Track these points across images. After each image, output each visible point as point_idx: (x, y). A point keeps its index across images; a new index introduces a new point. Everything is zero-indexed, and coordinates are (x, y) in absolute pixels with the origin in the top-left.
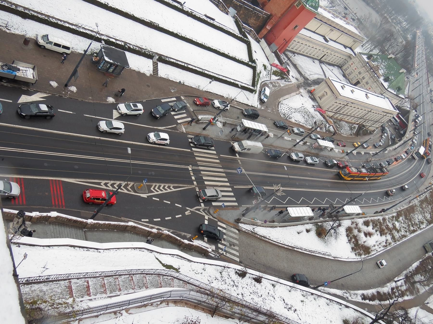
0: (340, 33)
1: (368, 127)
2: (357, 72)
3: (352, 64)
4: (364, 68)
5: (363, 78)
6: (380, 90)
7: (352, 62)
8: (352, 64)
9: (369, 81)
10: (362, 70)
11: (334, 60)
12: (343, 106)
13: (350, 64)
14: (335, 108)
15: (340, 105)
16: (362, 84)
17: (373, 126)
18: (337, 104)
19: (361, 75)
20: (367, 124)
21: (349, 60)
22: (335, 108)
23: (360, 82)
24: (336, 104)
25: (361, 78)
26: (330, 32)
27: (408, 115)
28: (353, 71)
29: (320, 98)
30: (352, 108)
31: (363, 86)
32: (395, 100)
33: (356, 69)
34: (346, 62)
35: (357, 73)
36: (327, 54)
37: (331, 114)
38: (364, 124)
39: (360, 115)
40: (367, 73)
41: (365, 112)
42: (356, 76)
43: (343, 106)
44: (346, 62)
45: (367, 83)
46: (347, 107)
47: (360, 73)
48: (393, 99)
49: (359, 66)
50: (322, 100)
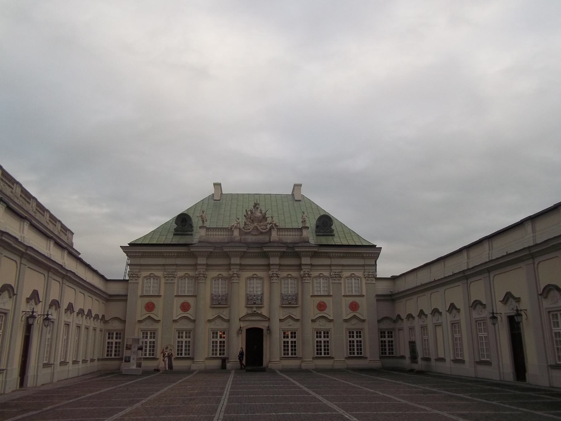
3: (150, 307)
4: (214, 274)
7: (141, 304)
8: (150, 307)
9: (289, 288)
13: (140, 313)
16: (276, 327)
21: (115, 309)
23: (263, 325)
25: (243, 311)
33: (185, 307)
34: (116, 325)
35: (211, 314)
45: (290, 302)
47: (221, 302)
49: (187, 287)
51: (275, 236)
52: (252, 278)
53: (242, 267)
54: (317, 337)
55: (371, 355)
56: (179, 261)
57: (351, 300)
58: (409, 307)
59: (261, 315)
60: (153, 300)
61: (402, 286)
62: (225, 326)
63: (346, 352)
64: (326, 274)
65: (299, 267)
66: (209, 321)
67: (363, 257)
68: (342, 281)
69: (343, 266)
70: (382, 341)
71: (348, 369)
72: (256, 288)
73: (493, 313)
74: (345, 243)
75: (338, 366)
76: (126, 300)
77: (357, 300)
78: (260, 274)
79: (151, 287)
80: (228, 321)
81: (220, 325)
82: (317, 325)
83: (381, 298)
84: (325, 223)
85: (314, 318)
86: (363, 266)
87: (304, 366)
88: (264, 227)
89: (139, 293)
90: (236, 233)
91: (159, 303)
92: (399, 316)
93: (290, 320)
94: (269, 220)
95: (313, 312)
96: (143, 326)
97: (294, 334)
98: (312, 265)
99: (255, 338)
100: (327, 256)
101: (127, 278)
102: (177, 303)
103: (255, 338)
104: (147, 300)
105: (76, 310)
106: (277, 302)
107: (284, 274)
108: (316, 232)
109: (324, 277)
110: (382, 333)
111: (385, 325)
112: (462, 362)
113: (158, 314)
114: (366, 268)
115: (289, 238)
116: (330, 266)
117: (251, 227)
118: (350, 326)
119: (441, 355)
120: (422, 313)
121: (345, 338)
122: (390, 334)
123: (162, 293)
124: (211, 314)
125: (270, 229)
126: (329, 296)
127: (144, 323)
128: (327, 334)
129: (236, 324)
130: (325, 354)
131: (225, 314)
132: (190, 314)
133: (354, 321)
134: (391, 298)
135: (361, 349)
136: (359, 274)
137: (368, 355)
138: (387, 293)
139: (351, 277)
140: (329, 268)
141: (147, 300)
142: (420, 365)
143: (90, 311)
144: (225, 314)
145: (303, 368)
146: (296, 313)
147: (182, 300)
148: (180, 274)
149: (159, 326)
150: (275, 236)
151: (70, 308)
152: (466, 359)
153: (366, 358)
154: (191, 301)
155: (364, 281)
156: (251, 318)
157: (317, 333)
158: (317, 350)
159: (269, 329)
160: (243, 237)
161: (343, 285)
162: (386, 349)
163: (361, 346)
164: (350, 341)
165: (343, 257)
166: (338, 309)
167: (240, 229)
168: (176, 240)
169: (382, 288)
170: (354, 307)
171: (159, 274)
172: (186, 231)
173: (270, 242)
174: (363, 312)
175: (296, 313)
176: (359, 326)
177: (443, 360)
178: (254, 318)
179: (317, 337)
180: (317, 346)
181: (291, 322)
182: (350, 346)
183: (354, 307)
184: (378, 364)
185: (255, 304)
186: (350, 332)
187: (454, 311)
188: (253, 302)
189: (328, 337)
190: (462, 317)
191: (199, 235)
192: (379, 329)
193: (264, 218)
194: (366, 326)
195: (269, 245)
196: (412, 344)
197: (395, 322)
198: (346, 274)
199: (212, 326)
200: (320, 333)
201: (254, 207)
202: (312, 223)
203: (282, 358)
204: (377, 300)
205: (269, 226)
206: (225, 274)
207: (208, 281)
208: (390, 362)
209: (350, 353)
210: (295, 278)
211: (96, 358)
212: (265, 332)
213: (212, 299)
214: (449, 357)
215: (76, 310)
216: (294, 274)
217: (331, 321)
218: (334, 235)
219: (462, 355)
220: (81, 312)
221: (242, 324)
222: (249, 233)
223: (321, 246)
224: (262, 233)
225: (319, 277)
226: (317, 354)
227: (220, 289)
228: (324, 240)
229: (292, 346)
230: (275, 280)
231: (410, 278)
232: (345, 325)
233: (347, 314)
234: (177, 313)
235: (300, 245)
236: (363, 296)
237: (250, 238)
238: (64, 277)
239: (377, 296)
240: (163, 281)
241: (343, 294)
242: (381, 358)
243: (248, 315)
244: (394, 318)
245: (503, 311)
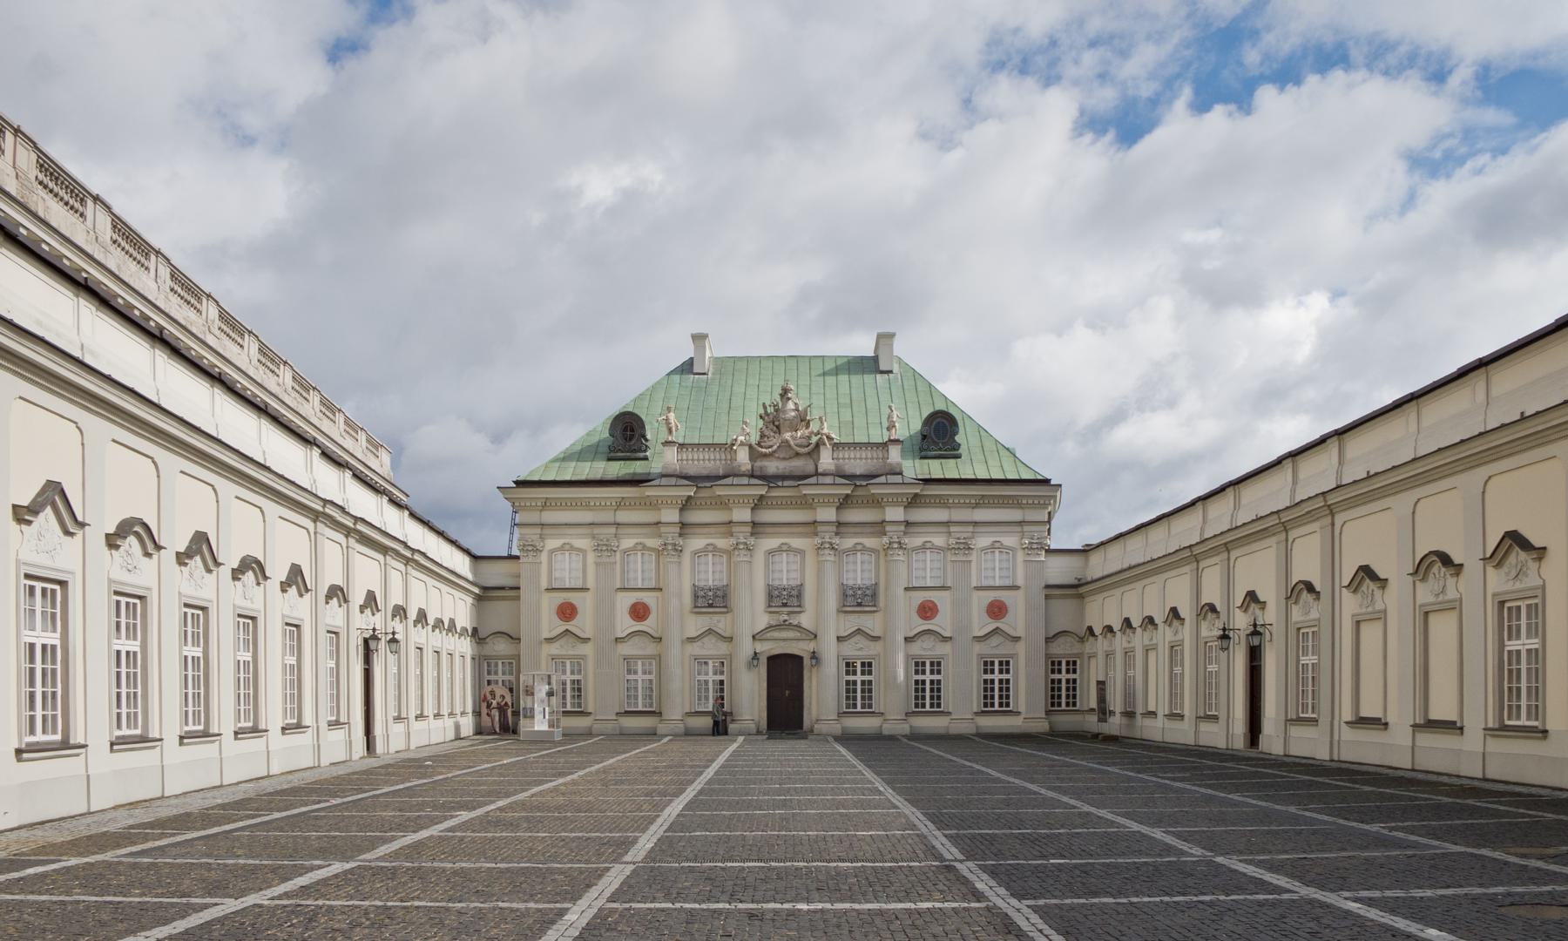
3: (567, 612)
4: (697, 543)
7: (549, 603)
8: (567, 612)
9: (859, 573)
10: (698, 565)
13: (550, 624)
16: (830, 651)
25: (763, 621)
33: (639, 612)
35: (695, 625)
42: (710, 648)
44: (501, 647)
45: (859, 600)
47: (713, 600)
49: (641, 570)
51: (826, 460)
52: (779, 550)
53: (757, 528)
54: (917, 672)
55: (1028, 708)
56: (624, 516)
57: (991, 596)
58: (1104, 610)
59: (798, 627)
60: (573, 598)
61: (1098, 566)
62: (723, 648)
63: (976, 703)
64: (939, 541)
65: (879, 527)
66: (691, 640)
67: (1020, 506)
68: (973, 557)
69: (976, 523)
70: (1053, 681)
71: (978, 735)
72: (786, 574)
73: (1255, 625)
74: (982, 474)
75: (957, 728)
76: (518, 598)
77: (1002, 595)
78: (796, 543)
79: (567, 570)
80: (730, 639)
81: (710, 648)
82: (917, 649)
83: (1053, 590)
84: (940, 431)
85: (912, 634)
86: (1021, 523)
87: (888, 729)
88: (804, 442)
89: (544, 584)
90: (743, 456)
91: (585, 604)
92: (1090, 629)
93: (858, 637)
94: (814, 427)
95: (905, 620)
96: (554, 649)
97: (867, 667)
98: (908, 524)
99: (785, 677)
100: (942, 503)
101: (515, 552)
102: (625, 601)
103: (785, 677)
104: (561, 597)
105: (431, 621)
106: (832, 601)
107: (849, 543)
108: (921, 450)
109: (934, 548)
110: (1054, 666)
111: (1062, 649)
112: (1182, 717)
113: (584, 623)
114: (1026, 528)
115: (858, 463)
116: (947, 524)
117: (775, 442)
118: (986, 649)
119: (1151, 708)
120: (1127, 623)
121: (976, 677)
122: (1072, 666)
123: (590, 583)
124: (695, 625)
125: (817, 445)
126: (943, 588)
127: (557, 645)
128: (936, 667)
129: (746, 648)
130: (932, 705)
132: (648, 625)
133: (995, 640)
134: (1077, 590)
135: (1008, 697)
136: (1010, 540)
137: (1022, 708)
138: (1070, 580)
139: (993, 547)
140: (944, 529)
141: (561, 597)
142: (1115, 725)
143: (452, 621)
144: (721, 623)
145: (885, 732)
146: (872, 623)
147: (630, 598)
148: (627, 543)
149: (587, 650)
151: (422, 617)
152: (1187, 713)
153: (1019, 713)
154: (648, 598)
155: (1020, 556)
156: (776, 634)
157: (917, 664)
158: (917, 698)
159: (814, 656)
160: (758, 464)
161: (974, 565)
162: (1059, 695)
163: (1008, 689)
164: (985, 681)
165: (977, 506)
166: (963, 616)
167: (750, 447)
168: (616, 469)
169: (1059, 570)
170: (997, 610)
171: (583, 543)
172: (635, 451)
173: (817, 474)
174: (1017, 620)
175: (872, 623)
176: (1006, 649)
177: (1153, 714)
178: (784, 634)
179: (917, 672)
180: (917, 690)
181: (859, 641)
182: (985, 690)
183: (997, 610)
184: (1042, 726)
185: (785, 605)
186: (986, 663)
187: (1176, 623)
188: (784, 599)
189: (939, 672)
190: (1186, 633)
191: (662, 459)
192: (1047, 656)
193: (803, 419)
194: (1020, 649)
195: (812, 480)
196: (1101, 685)
197: (1082, 640)
198: (983, 541)
199: (696, 649)
200: (924, 664)
201: (782, 396)
202: (910, 424)
203: (841, 714)
204: (1047, 597)
205: (814, 439)
206: (722, 543)
207: (686, 558)
208: (1065, 721)
209: (986, 705)
210: (873, 550)
212: (807, 662)
213: (696, 597)
214: (1163, 709)
215: (431, 621)
216: (870, 542)
217: (946, 639)
218: (958, 457)
219: (1182, 708)
220: (439, 623)
221: (760, 647)
222: (771, 455)
223: (927, 481)
224: (797, 454)
225: (923, 548)
226: (917, 706)
227: (711, 574)
228: (936, 468)
229: (863, 691)
230: (829, 556)
231: (1114, 551)
232: (978, 648)
233: (981, 624)
234: (625, 624)
235: (882, 479)
236: (1017, 588)
237: (772, 467)
238: (407, 561)
239: (1048, 587)
240: (591, 558)
241: (974, 584)
242: (1048, 713)
243: (770, 628)
244: (1083, 631)
245: (1241, 621)
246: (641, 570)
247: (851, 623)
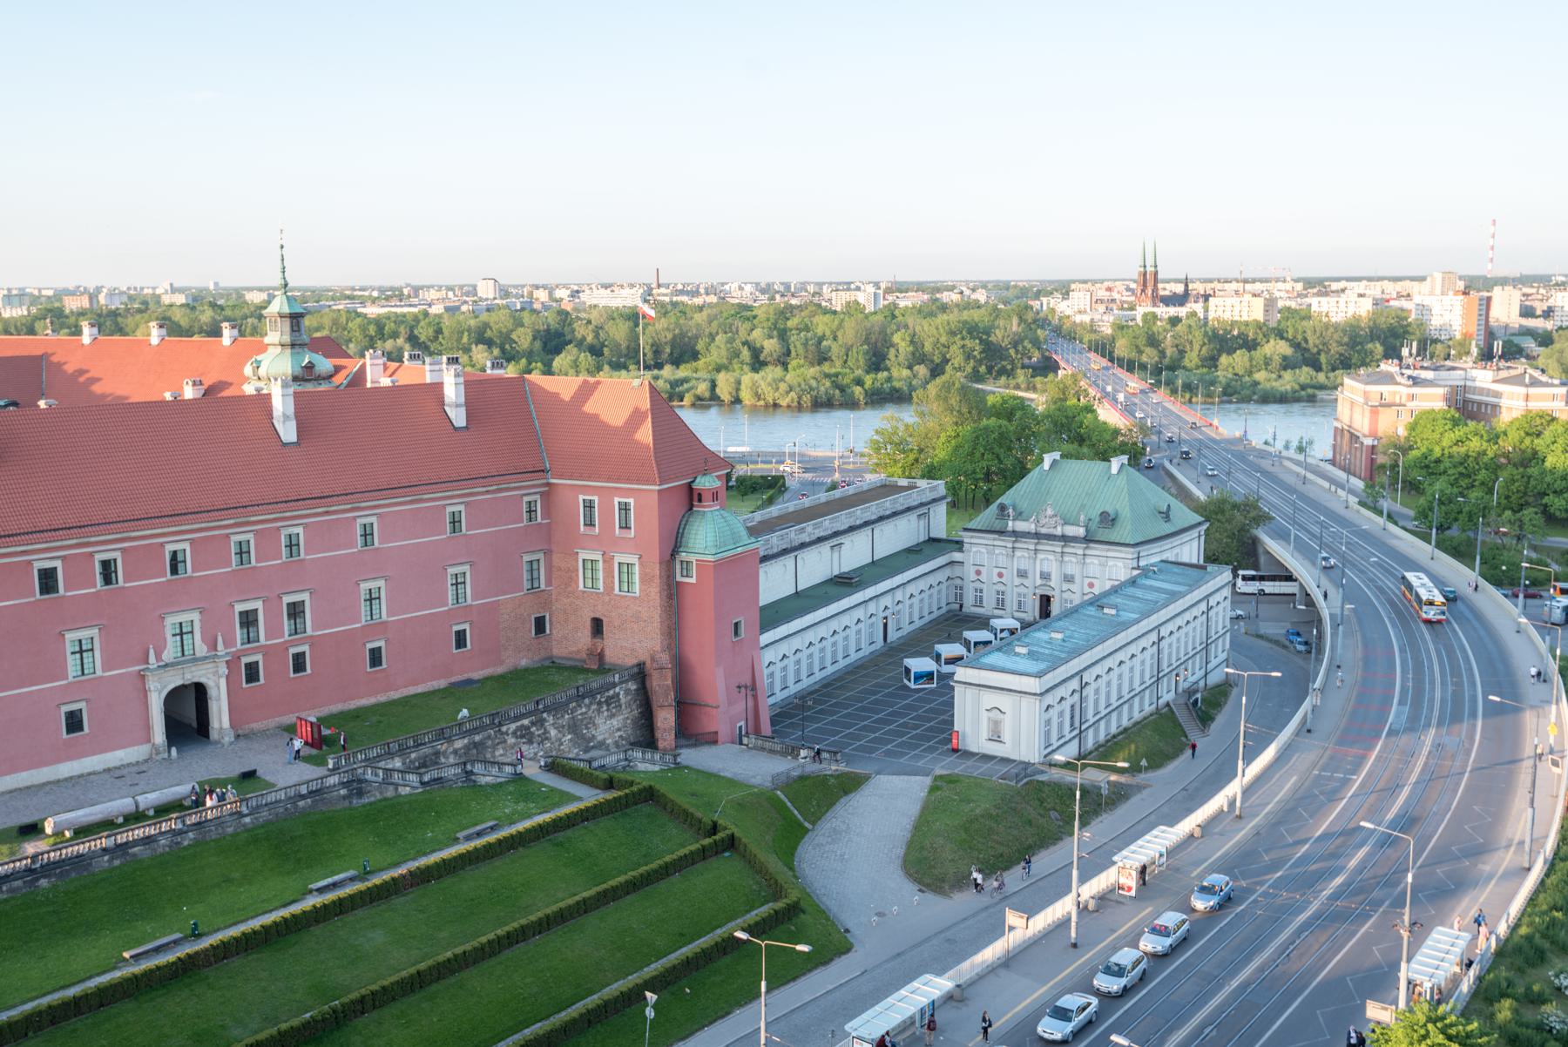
0: (867, 531)
1: (1202, 684)
2: (1011, 578)
3: (978, 573)
5: (1045, 576)
6: (1120, 564)
7: (973, 569)
8: (978, 573)
9: (1069, 570)
11: (921, 609)
12: (1077, 696)
13: (973, 577)
14: (1061, 725)
15: (1066, 705)
17: (1210, 666)
18: (1057, 708)
19: (1030, 575)
20: (1192, 679)
21: (957, 571)
22: (1061, 725)
24: (1053, 713)
25: (1039, 582)
26: (836, 555)
27: (1261, 550)
28: (1001, 588)
29: (996, 738)
30: (1105, 678)
31: (1065, 595)
32: (1186, 548)
33: (1000, 575)
34: (958, 582)
35: (1017, 581)
36: (887, 613)
37: (1072, 750)
38: (1183, 686)
39: (1147, 675)
40: (1041, 556)
41: (1147, 654)
42: (1022, 590)
43: (1077, 696)
45: (1069, 579)
46: (1089, 691)
47: (1022, 574)
48: (1177, 550)
49: (1002, 561)
50: (1007, 736)
81: (1022, 590)
99: (1046, 601)
102: (996, 571)
103: (1046, 601)
113: (983, 577)
129: (1031, 591)
131: (1026, 582)
144: (1026, 582)
150: (1059, 531)
198: (1111, 563)
211: (943, 604)
234: (996, 579)
237: (1044, 531)
246: (1002, 561)
247: (1065, 586)
